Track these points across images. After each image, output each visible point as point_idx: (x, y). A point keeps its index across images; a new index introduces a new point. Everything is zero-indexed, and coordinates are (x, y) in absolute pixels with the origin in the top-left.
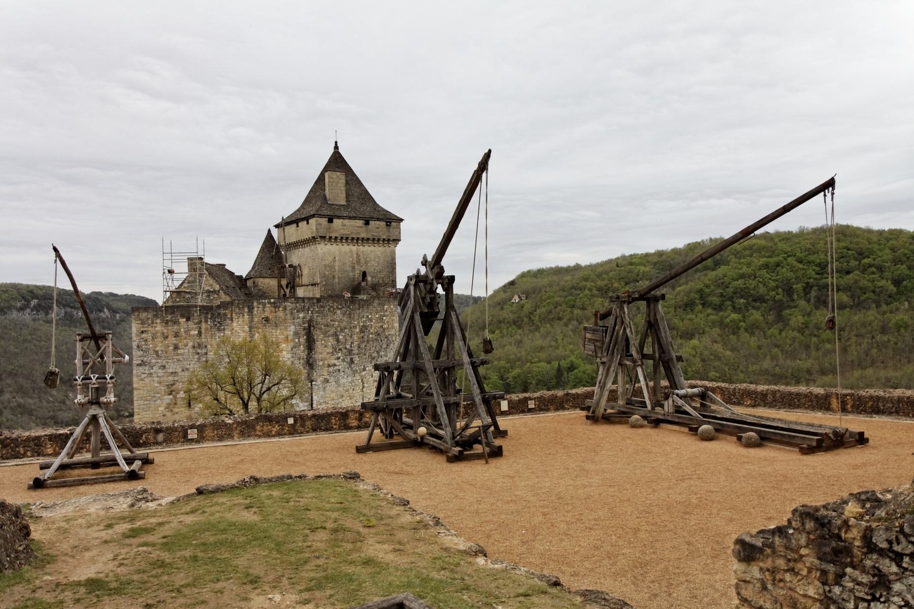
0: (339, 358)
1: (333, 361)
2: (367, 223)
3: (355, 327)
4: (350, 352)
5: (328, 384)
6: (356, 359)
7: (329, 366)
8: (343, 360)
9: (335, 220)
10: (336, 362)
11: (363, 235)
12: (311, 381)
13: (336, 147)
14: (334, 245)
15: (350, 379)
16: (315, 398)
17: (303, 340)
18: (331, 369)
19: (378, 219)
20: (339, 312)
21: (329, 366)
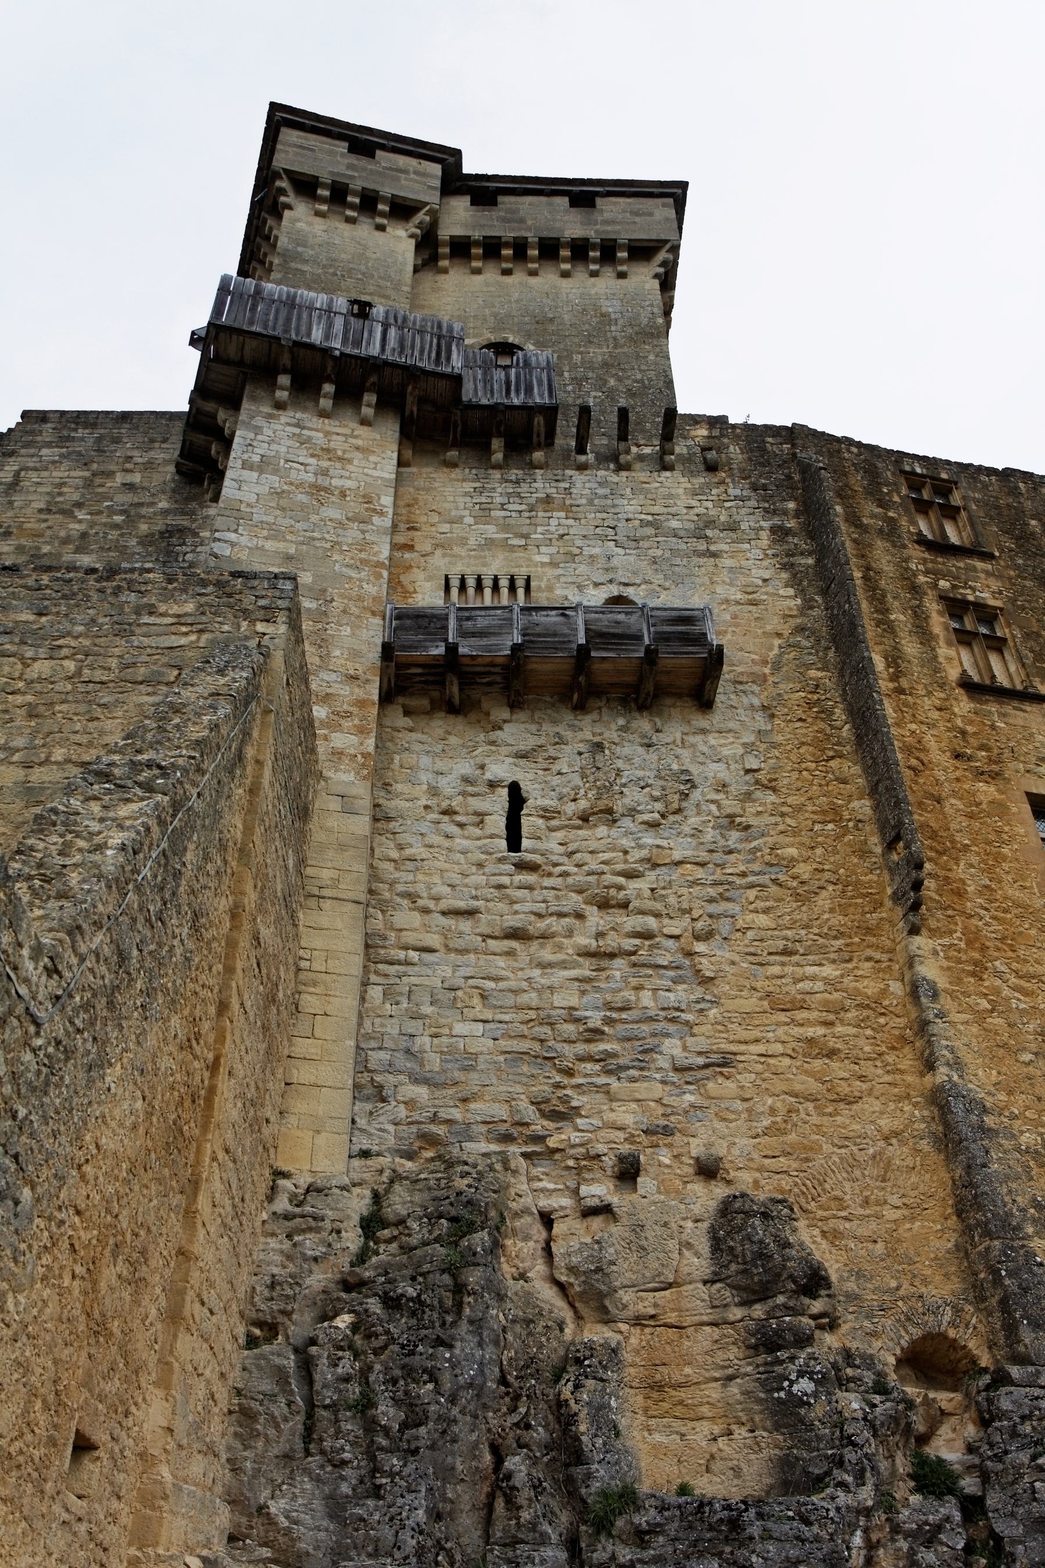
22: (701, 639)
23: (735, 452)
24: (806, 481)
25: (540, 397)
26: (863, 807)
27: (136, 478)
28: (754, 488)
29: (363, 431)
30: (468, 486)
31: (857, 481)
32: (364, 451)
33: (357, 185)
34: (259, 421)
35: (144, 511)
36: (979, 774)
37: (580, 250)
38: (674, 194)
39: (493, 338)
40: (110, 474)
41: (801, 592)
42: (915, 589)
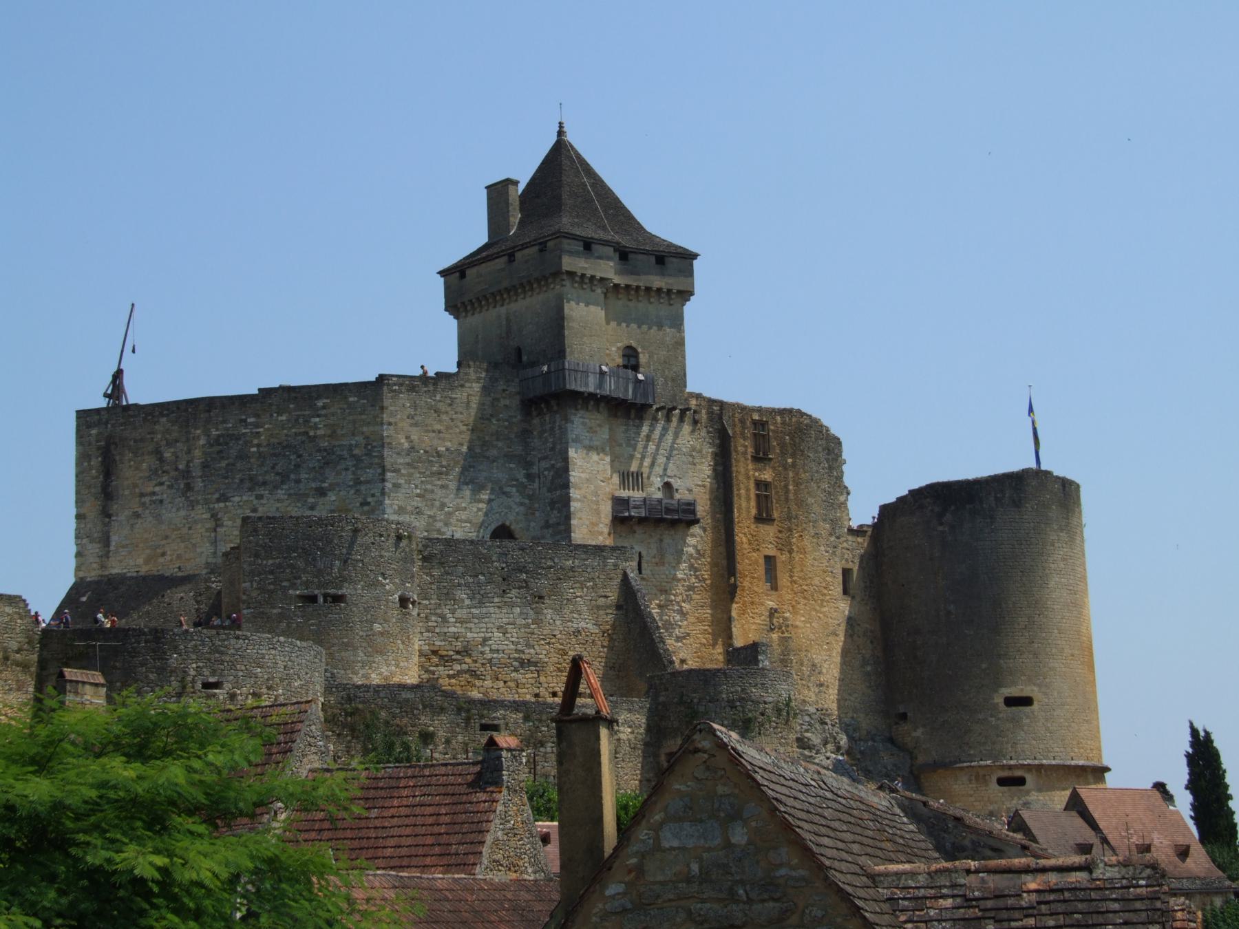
0: (161, 484)
1: (150, 489)
2: (511, 257)
3: (198, 438)
4: (186, 474)
5: (140, 521)
6: (199, 484)
7: (142, 495)
8: (170, 487)
9: (468, 272)
10: (157, 489)
11: (506, 284)
12: (109, 516)
13: (561, 133)
14: (476, 315)
15: (182, 513)
16: (114, 539)
17: (96, 461)
18: (147, 499)
19: (524, 246)
20: (164, 420)
21: (142, 495)
22: (694, 512)
23: (704, 416)
24: (725, 426)
25: (651, 401)
26: (724, 562)
27: (507, 402)
28: (709, 432)
29: (599, 416)
30: (623, 428)
31: (738, 429)
32: (600, 426)
33: (589, 273)
34: (573, 418)
35: (514, 420)
36: (754, 550)
37: (659, 290)
38: (695, 256)
39: (626, 343)
40: (498, 400)
41: (717, 482)
42: (748, 478)
